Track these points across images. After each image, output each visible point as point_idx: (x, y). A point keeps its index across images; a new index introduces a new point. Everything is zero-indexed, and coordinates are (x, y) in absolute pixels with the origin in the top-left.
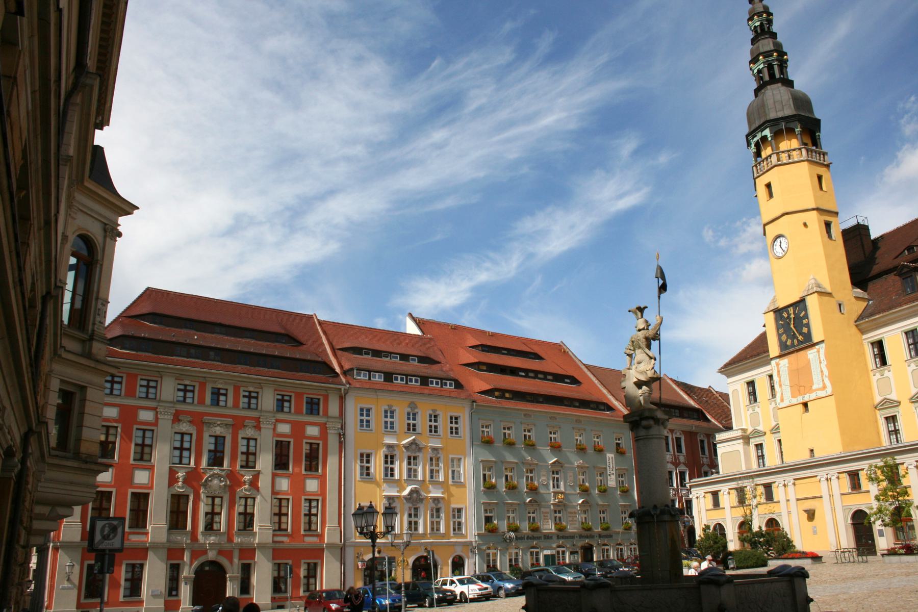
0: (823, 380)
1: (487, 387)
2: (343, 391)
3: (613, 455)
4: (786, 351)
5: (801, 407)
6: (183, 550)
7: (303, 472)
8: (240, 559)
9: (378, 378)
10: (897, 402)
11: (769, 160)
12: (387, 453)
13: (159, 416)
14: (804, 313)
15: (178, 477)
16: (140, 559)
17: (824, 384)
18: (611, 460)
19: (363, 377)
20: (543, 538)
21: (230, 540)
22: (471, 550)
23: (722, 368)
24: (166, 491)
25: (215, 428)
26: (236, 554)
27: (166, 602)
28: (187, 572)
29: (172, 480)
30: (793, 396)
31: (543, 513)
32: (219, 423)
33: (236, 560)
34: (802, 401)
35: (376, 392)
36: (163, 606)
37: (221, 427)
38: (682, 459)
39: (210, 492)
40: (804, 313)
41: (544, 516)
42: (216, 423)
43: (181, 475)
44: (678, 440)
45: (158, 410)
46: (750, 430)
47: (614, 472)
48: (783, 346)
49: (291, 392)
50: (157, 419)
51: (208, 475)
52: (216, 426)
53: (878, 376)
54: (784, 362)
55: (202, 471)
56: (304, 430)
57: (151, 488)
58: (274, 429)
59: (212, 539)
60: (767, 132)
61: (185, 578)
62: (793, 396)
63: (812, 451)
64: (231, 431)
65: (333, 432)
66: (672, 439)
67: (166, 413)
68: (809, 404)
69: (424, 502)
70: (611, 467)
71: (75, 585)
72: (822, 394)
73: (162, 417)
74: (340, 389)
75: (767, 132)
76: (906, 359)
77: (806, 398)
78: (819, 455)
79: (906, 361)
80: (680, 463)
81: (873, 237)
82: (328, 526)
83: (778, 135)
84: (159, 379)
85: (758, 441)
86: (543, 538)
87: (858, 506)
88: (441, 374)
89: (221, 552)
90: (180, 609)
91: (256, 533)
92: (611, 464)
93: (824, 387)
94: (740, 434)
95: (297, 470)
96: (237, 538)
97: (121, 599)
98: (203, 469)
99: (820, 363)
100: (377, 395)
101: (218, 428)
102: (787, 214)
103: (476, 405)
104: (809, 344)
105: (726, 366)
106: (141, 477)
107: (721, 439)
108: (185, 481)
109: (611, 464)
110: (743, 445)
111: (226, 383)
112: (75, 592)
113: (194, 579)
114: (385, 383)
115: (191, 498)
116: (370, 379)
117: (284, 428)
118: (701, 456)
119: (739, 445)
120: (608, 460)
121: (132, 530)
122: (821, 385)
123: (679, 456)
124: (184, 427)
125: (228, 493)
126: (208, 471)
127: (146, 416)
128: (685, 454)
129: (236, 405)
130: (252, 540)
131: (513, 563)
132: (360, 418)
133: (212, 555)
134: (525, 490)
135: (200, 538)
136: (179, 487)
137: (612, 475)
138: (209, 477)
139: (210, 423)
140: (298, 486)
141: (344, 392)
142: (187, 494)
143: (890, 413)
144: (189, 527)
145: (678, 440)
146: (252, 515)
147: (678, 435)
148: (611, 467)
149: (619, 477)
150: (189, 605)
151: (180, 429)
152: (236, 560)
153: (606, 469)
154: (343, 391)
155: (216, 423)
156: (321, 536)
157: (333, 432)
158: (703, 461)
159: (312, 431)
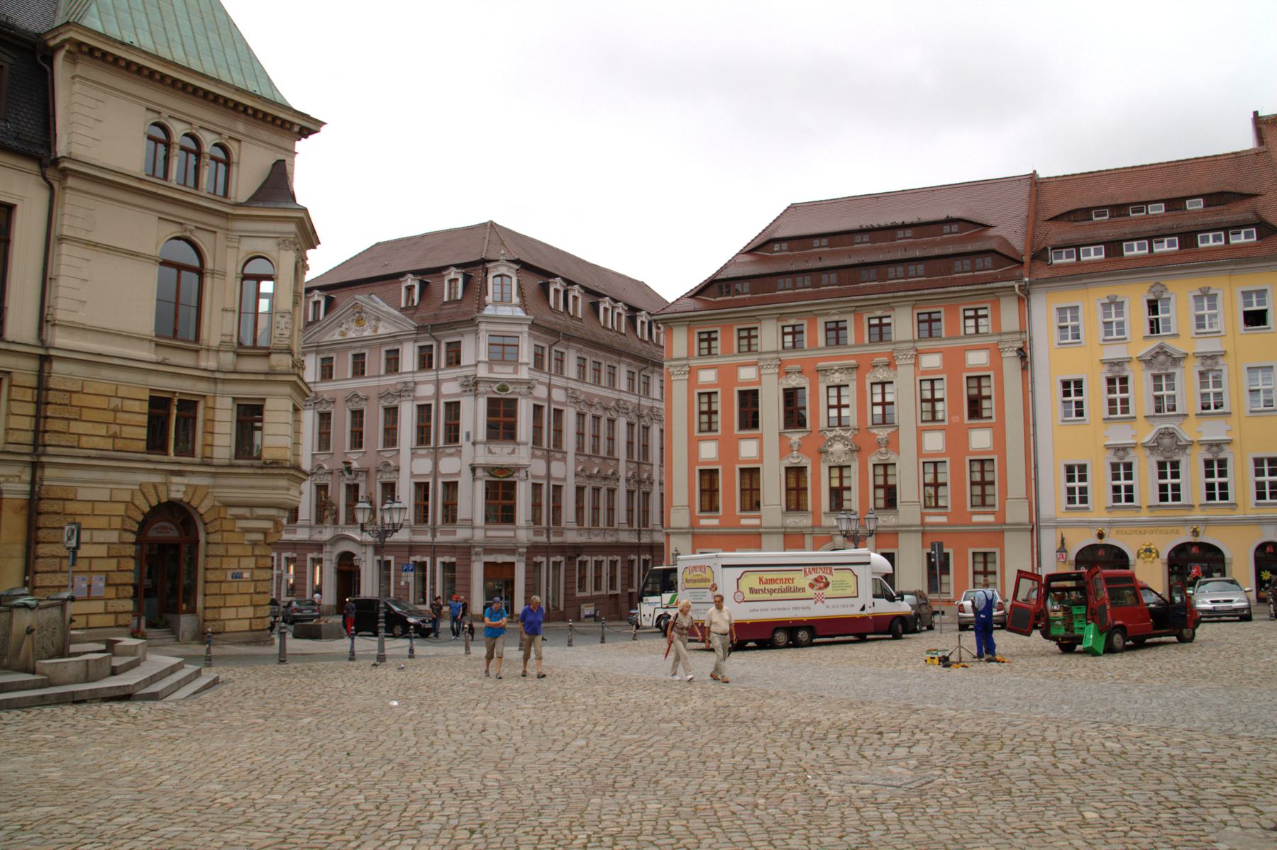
7: (966, 421)
9: (1093, 255)
32: (836, 368)
56: (964, 360)
58: (916, 364)
64: (854, 376)
69: (1188, 451)
74: (1013, 287)
95: (956, 419)
101: (837, 375)
111: (842, 313)
114: (1183, 251)
116: (1151, 250)
117: (931, 361)
140: (957, 440)
157: (1011, 354)
159: (977, 359)
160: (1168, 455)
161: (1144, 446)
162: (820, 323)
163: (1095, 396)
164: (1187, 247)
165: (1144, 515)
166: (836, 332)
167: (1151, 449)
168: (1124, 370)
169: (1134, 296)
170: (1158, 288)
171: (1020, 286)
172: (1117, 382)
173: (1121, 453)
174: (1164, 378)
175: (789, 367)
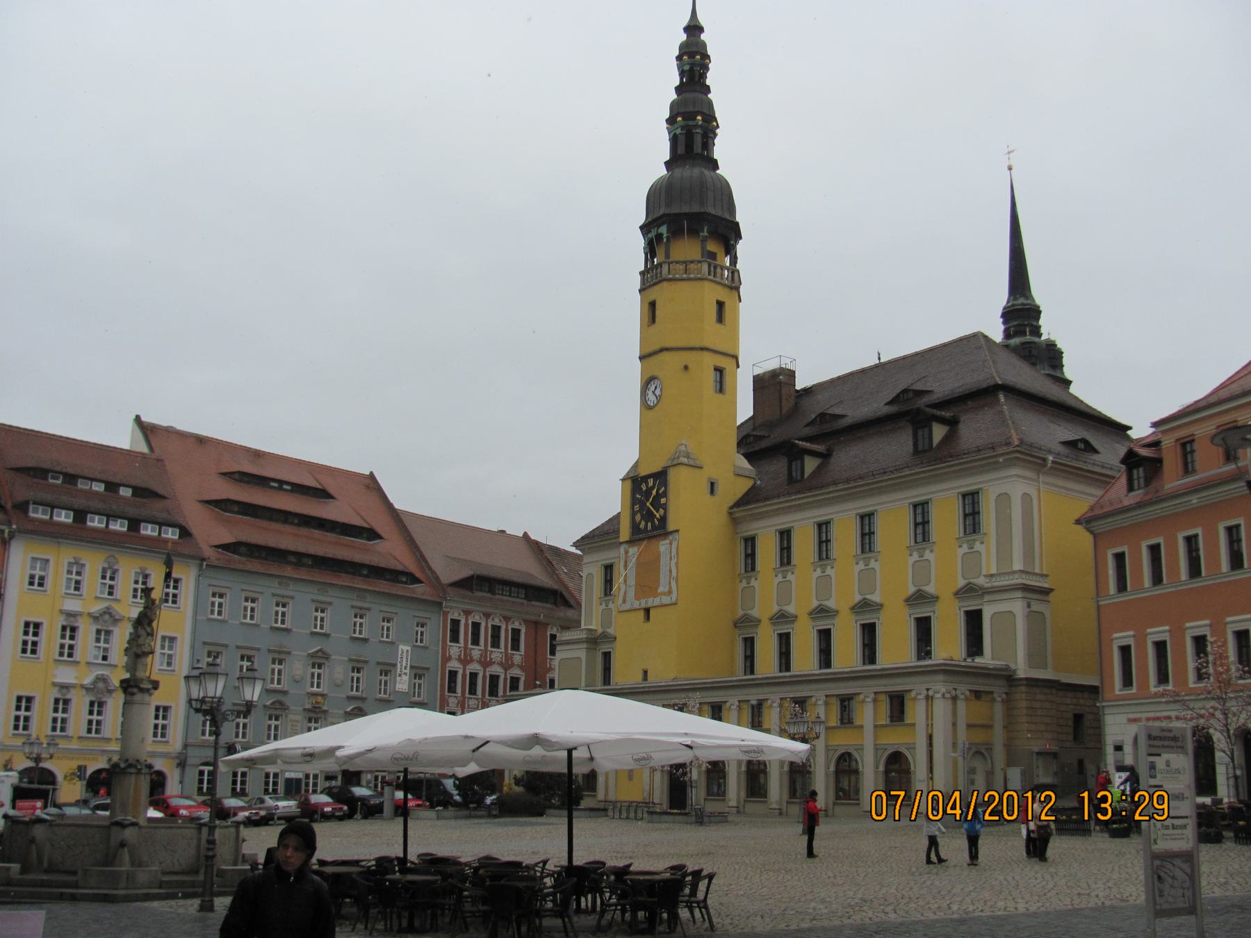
0: (670, 583)
1: (228, 538)
2: (6, 535)
3: (409, 648)
4: (638, 535)
5: (642, 614)
9: (64, 517)
10: (933, 597)
11: (659, 270)
12: (65, 623)
14: (663, 488)
17: (670, 587)
18: (405, 654)
19: (42, 514)
30: (637, 598)
31: (291, 721)
34: (643, 605)
38: (518, 658)
40: (663, 488)
41: (292, 725)
44: (516, 633)
46: (600, 631)
47: (408, 671)
48: (635, 527)
53: (744, 584)
54: (634, 551)
60: (663, 230)
62: (637, 598)
63: (645, 672)
66: (507, 630)
68: (652, 612)
70: (404, 665)
72: (666, 600)
75: (663, 230)
76: (908, 545)
77: (650, 605)
78: (653, 679)
79: (957, 539)
80: (512, 665)
81: (798, 387)
83: (676, 233)
85: (605, 648)
87: (752, 755)
88: (162, 516)
92: (404, 660)
93: (670, 592)
94: (585, 636)
99: (671, 559)
102: (667, 349)
103: (207, 565)
104: (662, 531)
107: (564, 639)
109: (404, 660)
110: (587, 652)
118: (549, 656)
119: (580, 653)
120: (400, 652)
122: (667, 589)
123: (513, 654)
128: (523, 653)
131: (239, 786)
132: (28, 572)
137: (404, 677)
141: (9, 535)
145: (516, 633)
147: (516, 625)
148: (404, 665)
149: (415, 678)
153: (395, 665)
154: (6, 535)
158: (550, 664)
160: (99, 696)
161: (82, 686)
163: (50, 639)
164: (132, 531)
165: (74, 745)
167: (87, 689)
168: (77, 621)
169: (94, 562)
170: (111, 560)
171: (9, 532)
172: (70, 630)
173: (64, 691)
174: (103, 633)
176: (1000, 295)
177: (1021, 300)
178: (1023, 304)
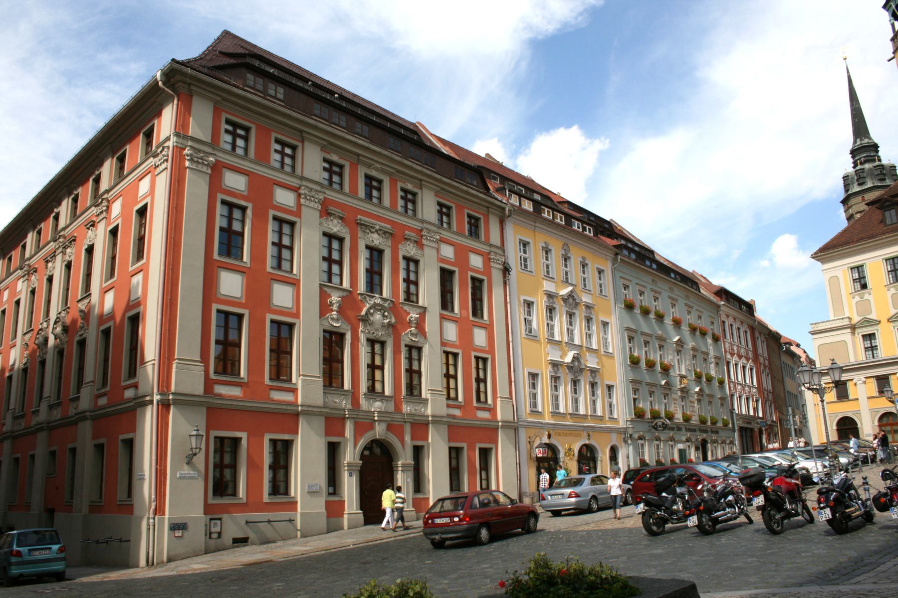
6: (343, 419)
8: (412, 439)
13: (302, 201)
15: (331, 302)
16: (289, 432)
20: (676, 429)
21: (398, 408)
22: (624, 439)
23: (816, 253)
24: (318, 323)
25: (372, 235)
26: (408, 429)
27: (328, 503)
28: (350, 455)
29: (325, 308)
33: (408, 438)
35: (535, 222)
36: (324, 510)
37: (379, 234)
39: (372, 332)
42: (374, 228)
43: (335, 298)
45: (302, 191)
49: (453, 203)
50: (299, 205)
51: (368, 306)
52: (373, 232)
55: (359, 298)
57: (297, 315)
59: (377, 406)
61: (349, 465)
64: (389, 243)
65: (497, 266)
67: (313, 199)
71: (199, 471)
73: (307, 203)
82: (501, 397)
84: (300, 145)
86: (676, 429)
89: (390, 428)
90: (346, 516)
91: (427, 400)
96: (405, 406)
97: (266, 498)
98: (361, 294)
100: (535, 226)
101: (375, 236)
105: (821, 250)
106: (282, 296)
108: (340, 311)
112: (200, 484)
113: (361, 467)
115: (348, 337)
117: (448, 252)
121: (275, 384)
124: (335, 227)
125: (392, 336)
126: (368, 298)
127: (284, 198)
129: (393, 208)
130: (423, 410)
133: (379, 431)
134: (660, 369)
135: (364, 403)
136: (333, 319)
138: (370, 308)
139: (366, 226)
142: (342, 331)
143: (868, 331)
144: (347, 385)
146: (419, 373)
150: (356, 510)
151: (329, 228)
152: (408, 438)
155: (374, 228)
156: (492, 410)
162: (362, 171)
166: (373, 185)
175: (332, 209)
176: (846, 138)
177: (866, 140)
178: (868, 143)
